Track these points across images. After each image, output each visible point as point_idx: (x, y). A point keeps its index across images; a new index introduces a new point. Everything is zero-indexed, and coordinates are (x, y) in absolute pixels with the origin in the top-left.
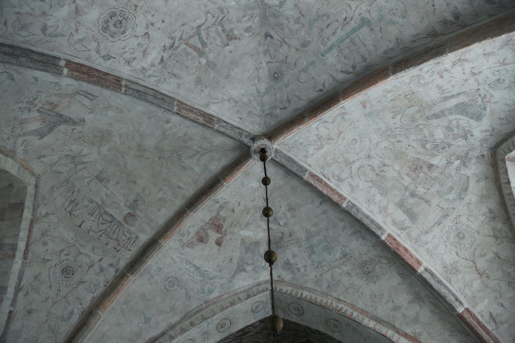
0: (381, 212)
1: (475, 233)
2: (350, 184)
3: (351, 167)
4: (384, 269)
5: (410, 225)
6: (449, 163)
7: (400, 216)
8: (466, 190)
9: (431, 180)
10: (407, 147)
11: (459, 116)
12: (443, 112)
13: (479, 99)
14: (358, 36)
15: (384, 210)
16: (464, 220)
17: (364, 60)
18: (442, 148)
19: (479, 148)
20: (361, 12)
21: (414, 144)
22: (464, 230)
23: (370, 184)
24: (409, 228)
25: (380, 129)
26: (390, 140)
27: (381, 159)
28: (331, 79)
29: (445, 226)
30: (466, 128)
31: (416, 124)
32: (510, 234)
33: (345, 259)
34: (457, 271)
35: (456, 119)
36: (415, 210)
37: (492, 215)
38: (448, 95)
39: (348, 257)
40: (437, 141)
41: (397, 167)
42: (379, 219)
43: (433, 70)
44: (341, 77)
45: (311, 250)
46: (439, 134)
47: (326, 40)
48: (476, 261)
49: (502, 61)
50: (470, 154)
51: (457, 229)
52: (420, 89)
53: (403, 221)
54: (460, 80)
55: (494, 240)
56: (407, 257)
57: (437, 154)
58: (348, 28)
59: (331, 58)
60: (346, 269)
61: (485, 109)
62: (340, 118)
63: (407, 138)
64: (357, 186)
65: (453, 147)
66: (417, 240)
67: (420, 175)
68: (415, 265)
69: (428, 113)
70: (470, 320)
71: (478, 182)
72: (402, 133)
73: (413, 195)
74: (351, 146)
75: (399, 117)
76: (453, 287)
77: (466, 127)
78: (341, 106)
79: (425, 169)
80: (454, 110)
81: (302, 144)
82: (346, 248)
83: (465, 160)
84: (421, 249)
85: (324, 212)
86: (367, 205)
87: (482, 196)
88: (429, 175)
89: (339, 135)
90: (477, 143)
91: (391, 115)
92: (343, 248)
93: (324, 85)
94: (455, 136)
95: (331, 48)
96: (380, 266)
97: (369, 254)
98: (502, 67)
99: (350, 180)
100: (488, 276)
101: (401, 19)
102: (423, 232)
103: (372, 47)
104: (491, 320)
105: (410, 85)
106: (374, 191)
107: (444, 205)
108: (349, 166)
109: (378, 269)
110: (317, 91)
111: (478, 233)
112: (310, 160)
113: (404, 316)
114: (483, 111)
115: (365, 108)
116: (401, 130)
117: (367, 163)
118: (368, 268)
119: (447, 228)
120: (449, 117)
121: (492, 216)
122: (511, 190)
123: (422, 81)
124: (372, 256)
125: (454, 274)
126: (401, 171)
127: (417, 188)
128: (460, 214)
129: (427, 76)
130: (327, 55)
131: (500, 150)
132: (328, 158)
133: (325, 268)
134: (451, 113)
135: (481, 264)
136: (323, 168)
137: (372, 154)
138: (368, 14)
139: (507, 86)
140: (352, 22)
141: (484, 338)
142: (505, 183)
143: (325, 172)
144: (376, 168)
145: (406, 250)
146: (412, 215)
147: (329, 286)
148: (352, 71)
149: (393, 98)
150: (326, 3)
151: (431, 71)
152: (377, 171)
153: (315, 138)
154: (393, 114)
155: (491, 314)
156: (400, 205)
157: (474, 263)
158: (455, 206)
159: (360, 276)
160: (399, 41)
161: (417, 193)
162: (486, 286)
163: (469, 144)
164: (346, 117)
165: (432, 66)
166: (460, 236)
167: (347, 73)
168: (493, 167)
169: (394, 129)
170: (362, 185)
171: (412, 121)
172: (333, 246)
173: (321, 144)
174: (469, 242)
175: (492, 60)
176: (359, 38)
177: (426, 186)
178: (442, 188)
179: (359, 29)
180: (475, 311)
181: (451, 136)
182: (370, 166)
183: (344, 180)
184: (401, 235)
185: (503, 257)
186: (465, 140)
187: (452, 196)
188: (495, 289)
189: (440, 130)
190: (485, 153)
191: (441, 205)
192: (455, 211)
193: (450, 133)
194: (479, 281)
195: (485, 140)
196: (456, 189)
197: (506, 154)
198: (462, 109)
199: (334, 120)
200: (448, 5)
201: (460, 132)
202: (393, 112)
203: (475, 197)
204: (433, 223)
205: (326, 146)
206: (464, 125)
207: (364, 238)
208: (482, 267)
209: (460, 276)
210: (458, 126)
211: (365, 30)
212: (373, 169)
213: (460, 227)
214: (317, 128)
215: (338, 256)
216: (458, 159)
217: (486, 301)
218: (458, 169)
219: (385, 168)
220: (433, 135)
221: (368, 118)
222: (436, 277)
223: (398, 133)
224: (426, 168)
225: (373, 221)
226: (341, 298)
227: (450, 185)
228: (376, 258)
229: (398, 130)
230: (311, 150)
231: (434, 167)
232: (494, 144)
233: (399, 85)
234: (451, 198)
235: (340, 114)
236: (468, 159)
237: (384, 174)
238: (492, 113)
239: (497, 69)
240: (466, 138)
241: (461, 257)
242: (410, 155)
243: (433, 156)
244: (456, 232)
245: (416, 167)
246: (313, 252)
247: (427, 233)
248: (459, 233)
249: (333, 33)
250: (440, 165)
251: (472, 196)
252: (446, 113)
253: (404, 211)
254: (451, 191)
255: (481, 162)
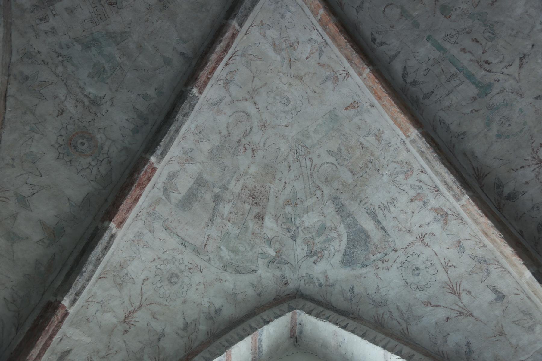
0: (185, 153)
1: (182, 298)
2: (221, 100)
3: (246, 100)
4: (87, 170)
5: (173, 200)
6: (270, 242)
7: (184, 183)
8: (238, 272)
9: (243, 222)
10: (283, 180)
11: (345, 239)
12: (350, 215)
13: (379, 255)
14: (462, 82)
15: (188, 157)
16: (197, 278)
17: (427, 96)
18: (288, 229)
19: (296, 276)
20: (501, 81)
21: (289, 189)
22: (182, 283)
23: (224, 132)
24: (169, 199)
25: (308, 137)
26: (290, 155)
27: (262, 145)
28: (392, 53)
29: (182, 253)
30: (326, 252)
31: (321, 185)
32: (197, 344)
33: (87, 103)
34: (120, 286)
35: (339, 235)
36: (196, 205)
37: (213, 314)
38: (380, 216)
39: (94, 109)
40: (298, 219)
41: (253, 170)
42: (174, 151)
43: (423, 186)
44: (398, 66)
45: (90, 43)
46: (311, 220)
47: (453, 40)
48: (143, 309)
49: (449, 264)
50: (286, 266)
51: (182, 272)
52: (385, 178)
53: (177, 190)
54: (409, 225)
55: (182, 326)
56: (128, 201)
57: (280, 222)
58: (473, 69)
59: (425, 51)
60: (70, 105)
61: (364, 266)
62: (328, 74)
63: (296, 178)
64: (219, 112)
65: (291, 242)
66: (152, 215)
67: (246, 205)
68: (118, 218)
69: (344, 198)
70: (55, 320)
71: (252, 284)
72: (304, 170)
73: (217, 199)
74: (278, 98)
75: (332, 159)
76: (94, 285)
77: (329, 251)
78: (352, 71)
79: (256, 210)
80: (355, 229)
81: (283, 17)
82: (109, 103)
83: (277, 261)
84: (140, 224)
85: (167, 62)
86: (193, 129)
87: (234, 295)
88: (249, 217)
89: (296, 77)
90: (303, 272)
91: (335, 148)
92: (107, 98)
93: (382, 44)
94: (311, 241)
95: (440, 48)
96: (93, 163)
97: (108, 143)
98: (440, 268)
99: (228, 99)
100: (126, 331)
101: (496, 133)
102: (166, 223)
103: (447, 104)
104: (59, 355)
105: (394, 164)
106: (216, 140)
107: (212, 246)
108: (248, 97)
109: (84, 161)
110: (372, 34)
111: (184, 302)
112: (255, 32)
113: (14, 217)
114: (359, 265)
115: (347, 108)
116: (309, 167)
117: (255, 124)
118: (82, 144)
119: (180, 256)
120: (342, 226)
121: (212, 316)
122: (260, 328)
123: (401, 177)
124: (106, 148)
125: (114, 282)
126: (248, 176)
127: (228, 203)
128: (204, 271)
129: (412, 181)
130: (429, 45)
131: (302, 302)
132: (259, 62)
133: (60, 69)
134: (348, 226)
135: (142, 318)
136: (243, 55)
137: (269, 130)
138: (498, 91)
139: (409, 281)
140: (483, 72)
141: (33, 351)
142: (262, 319)
143: (237, 59)
144: (248, 139)
145: (136, 200)
146: (188, 201)
147: (27, 78)
148: (409, 81)
149: (366, 144)
150: (514, 32)
151: (421, 184)
152: (244, 141)
153: (293, 39)
154: (336, 151)
155: (68, 352)
156: (200, 182)
157: (141, 306)
158: (213, 262)
159: (63, 132)
160: (462, 136)
161: (221, 204)
162: (111, 332)
163: (301, 262)
164: (330, 84)
165: (430, 183)
166: (173, 278)
167: (405, 75)
168: (275, 299)
169: (310, 156)
170: (223, 120)
171: (327, 179)
172: (108, 81)
173: (281, 50)
174: (168, 292)
175: (452, 254)
176: (459, 85)
177: (232, 216)
178: (235, 239)
179: (474, 83)
180: (65, 326)
181: (310, 235)
182: (251, 129)
183: (227, 90)
184: (156, 190)
185: (161, 343)
186: (305, 255)
187: (225, 254)
188: (111, 346)
189: (316, 220)
190: (291, 285)
191: (211, 241)
192: (207, 263)
193: (314, 234)
194: (115, 321)
195: (310, 279)
196: (237, 257)
197: (302, 309)
198: (359, 238)
199: (323, 66)
200: (527, 183)
201: (319, 245)
202: (339, 150)
203: (232, 286)
204: (182, 235)
205: (278, 58)
206: (332, 248)
207: (136, 131)
208: (137, 320)
209: (115, 292)
210: (328, 240)
211: (473, 91)
212: (246, 134)
213: (186, 274)
214: (310, 40)
215: (91, 90)
216: (276, 252)
217: (86, 339)
218: (264, 255)
219: (249, 152)
220: (306, 211)
221: (327, 116)
222: (104, 255)
223: (303, 164)
224: (258, 211)
225: (172, 140)
226: (10, 101)
227: (240, 248)
228: (105, 156)
229: (309, 163)
230: (272, 34)
231: (261, 222)
232: (308, 293)
233: (392, 148)
234: (223, 254)
235: (334, 73)
236: (278, 265)
237: (242, 151)
238: (360, 276)
239: (436, 262)
240: (308, 256)
241: (144, 287)
242: (273, 186)
243: (276, 218)
244: (177, 271)
245: (257, 197)
246: (87, 47)
247: (166, 228)
248: (177, 276)
249: (464, 49)
250: (264, 230)
251: (231, 281)
252: (348, 220)
253: (191, 188)
254: (233, 251)
255: (278, 283)
